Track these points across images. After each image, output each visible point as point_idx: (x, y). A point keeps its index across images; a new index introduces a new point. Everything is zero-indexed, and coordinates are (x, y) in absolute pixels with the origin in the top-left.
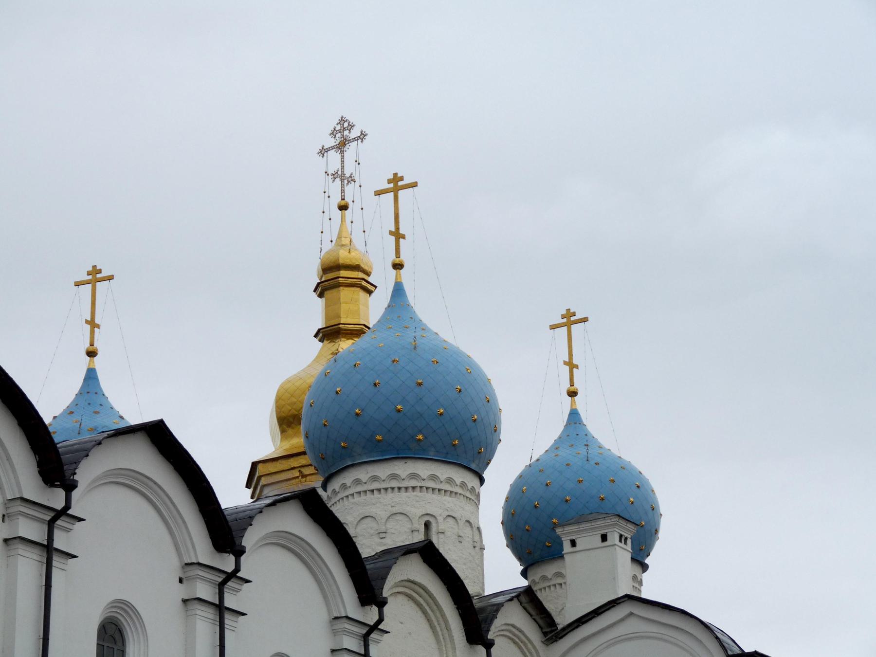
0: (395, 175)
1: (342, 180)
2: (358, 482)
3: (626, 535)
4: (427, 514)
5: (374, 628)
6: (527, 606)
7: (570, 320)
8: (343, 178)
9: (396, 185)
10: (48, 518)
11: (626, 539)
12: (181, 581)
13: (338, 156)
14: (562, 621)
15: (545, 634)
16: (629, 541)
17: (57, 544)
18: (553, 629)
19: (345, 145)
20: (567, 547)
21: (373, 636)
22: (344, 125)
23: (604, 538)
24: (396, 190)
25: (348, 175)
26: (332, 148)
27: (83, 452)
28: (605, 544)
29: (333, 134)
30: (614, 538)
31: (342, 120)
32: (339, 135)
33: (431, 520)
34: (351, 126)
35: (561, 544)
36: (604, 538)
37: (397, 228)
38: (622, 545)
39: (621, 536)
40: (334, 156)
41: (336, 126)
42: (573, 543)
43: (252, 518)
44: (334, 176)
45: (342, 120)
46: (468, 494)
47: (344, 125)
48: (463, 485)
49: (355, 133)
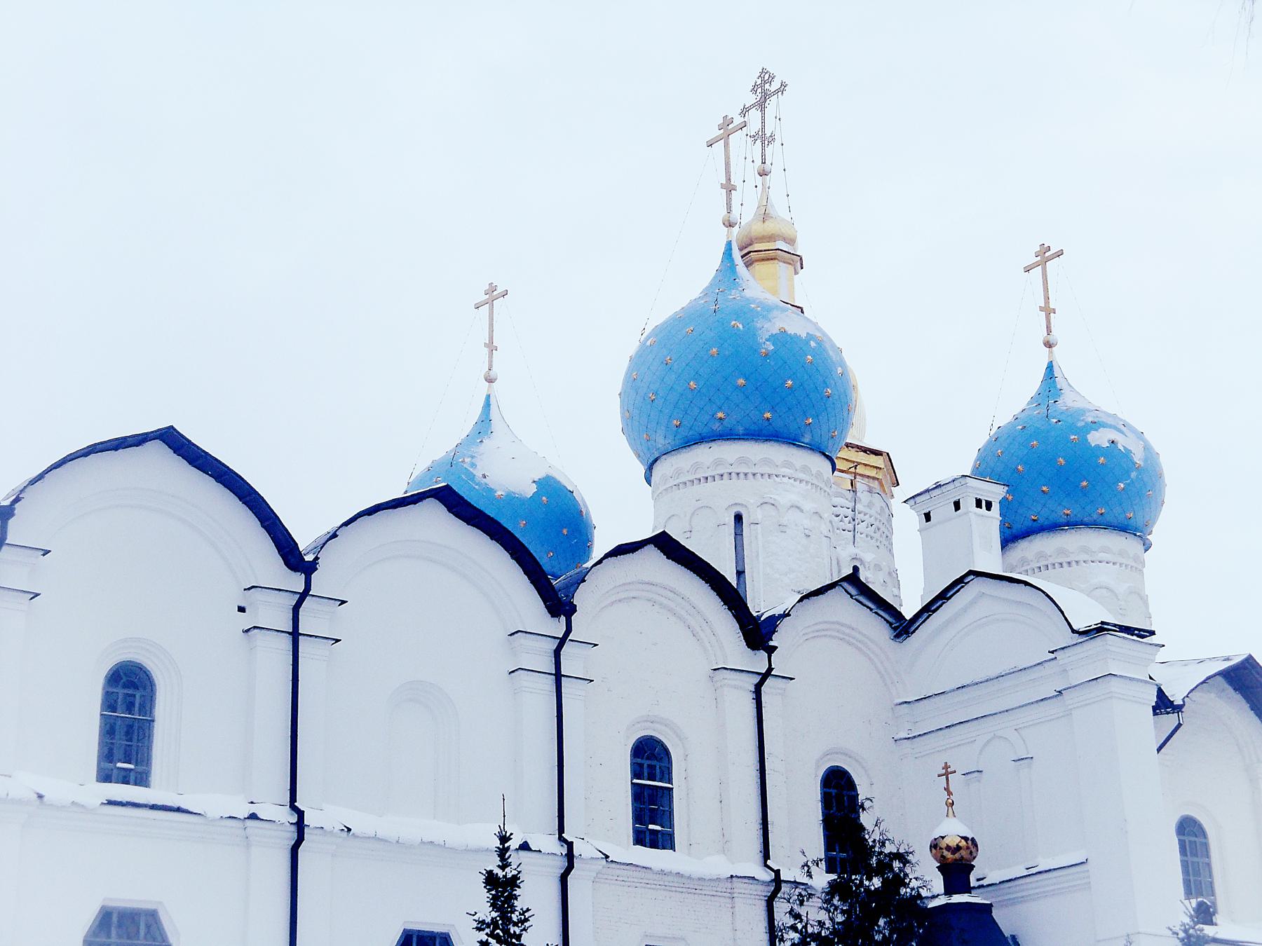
4: (736, 504)
6: (861, 598)
7: (1045, 256)
14: (908, 613)
15: (895, 629)
16: (996, 507)
18: (902, 622)
22: (766, 77)
23: (957, 505)
25: (768, 135)
29: (754, 90)
32: (759, 90)
34: (772, 78)
36: (957, 505)
39: (978, 503)
41: (757, 80)
45: (763, 71)
47: (766, 77)
49: (775, 85)
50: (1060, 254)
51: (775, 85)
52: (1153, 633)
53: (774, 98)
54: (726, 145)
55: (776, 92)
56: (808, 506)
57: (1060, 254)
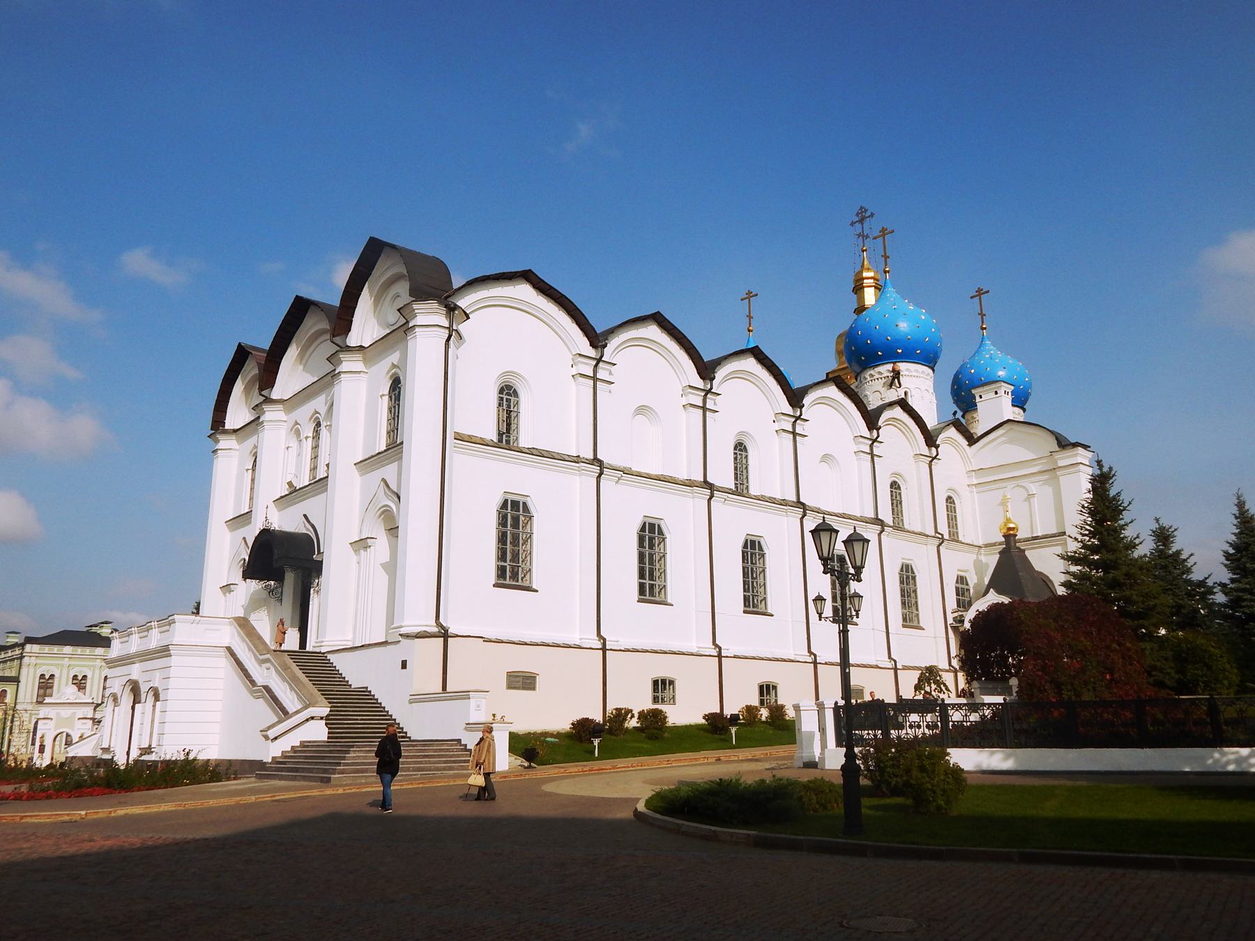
0: (883, 228)
1: (863, 237)
2: (872, 376)
3: (1007, 391)
5: (875, 441)
7: (980, 292)
8: (863, 236)
9: (884, 232)
10: (703, 394)
12: (774, 422)
13: (860, 225)
16: (1010, 394)
17: (708, 406)
19: (863, 220)
20: (978, 399)
21: (875, 444)
22: (863, 210)
23: (996, 393)
24: (884, 236)
26: (857, 222)
27: (718, 363)
28: (997, 396)
29: (857, 215)
30: (1001, 392)
31: (862, 208)
33: (908, 390)
34: (866, 211)
35: (975, 398)
36: (996, 393)
37: (885, 253)
38: (1006, 395)
40: (858, 225)
42: (981, 397)
43: (807, 391)
44: (859, 235)
45: (862, 208)
46: (926, 377)
47: (863, 210)
48: (923, 372)
49: (868, 214)
51: (868, 214)
52: (1089, 447)
53: (868, 219)
54: (884, 238)
55: (869, 217)
56: (923, 388)
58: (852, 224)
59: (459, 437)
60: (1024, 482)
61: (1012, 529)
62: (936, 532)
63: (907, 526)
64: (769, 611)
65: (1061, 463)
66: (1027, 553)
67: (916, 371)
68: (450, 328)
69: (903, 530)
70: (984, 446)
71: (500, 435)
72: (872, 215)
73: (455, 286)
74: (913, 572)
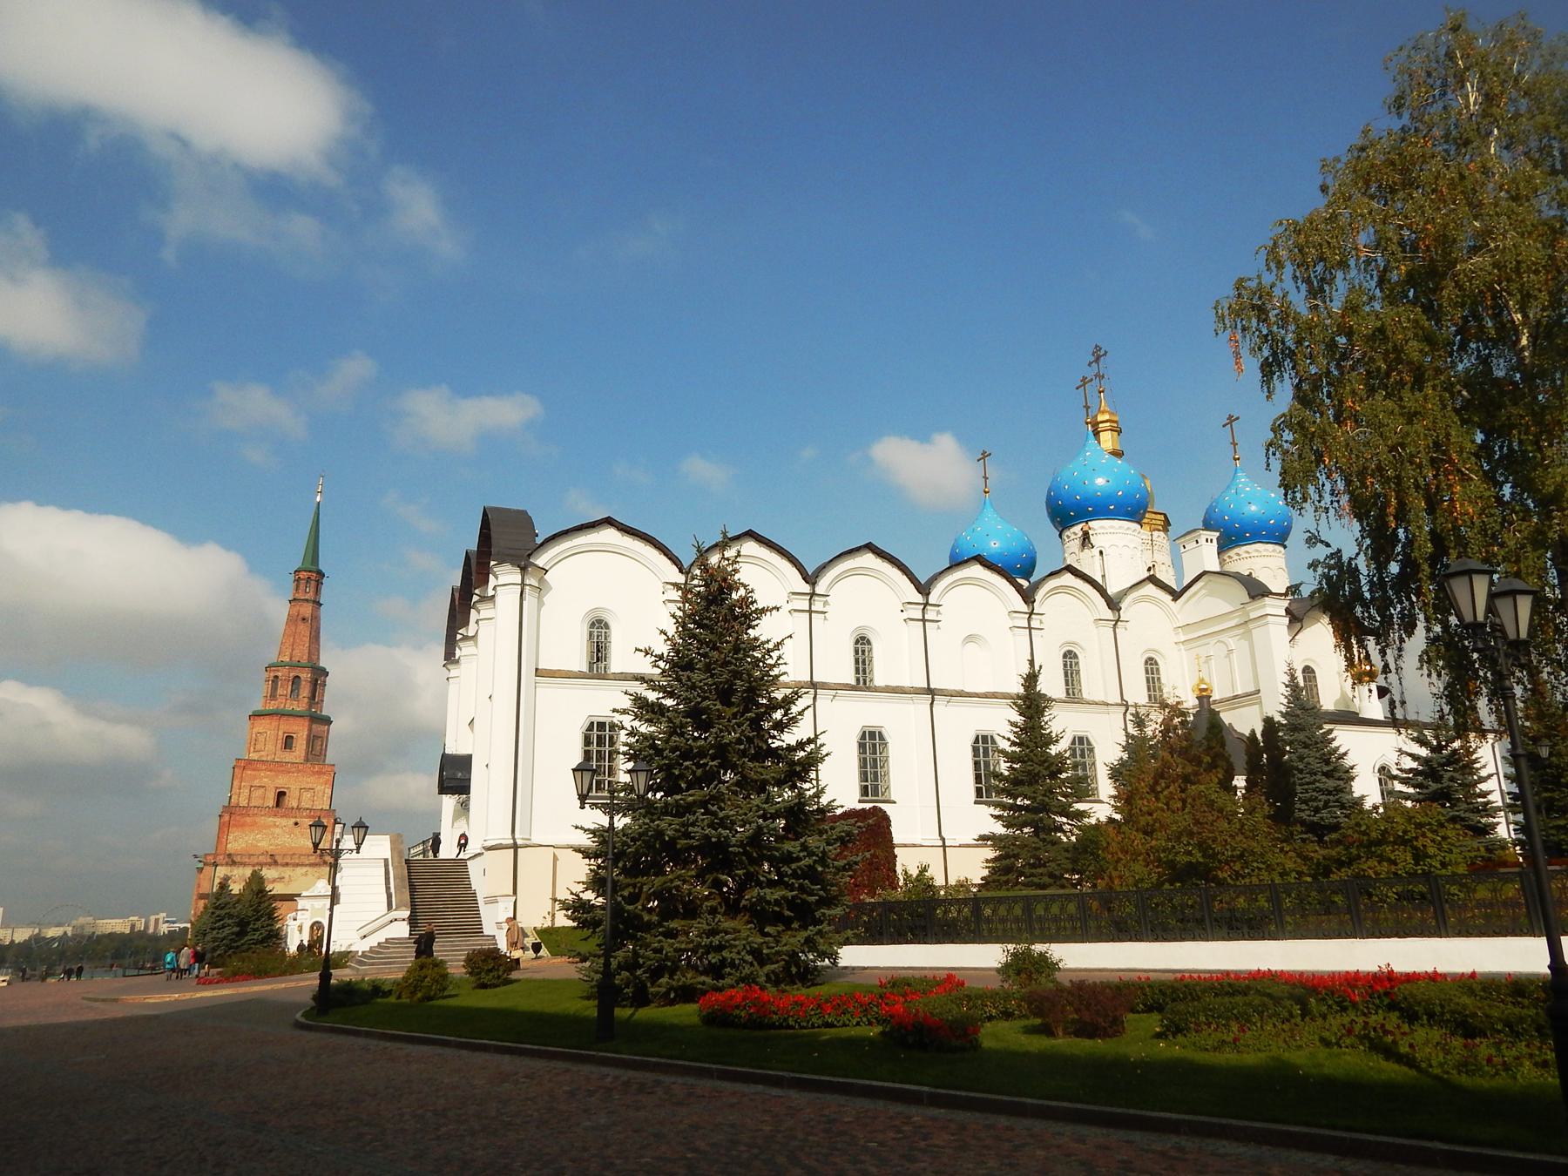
11: (1211, 541)
16: (1215, 541)
22: (1098, 348)
30: (1202, 540)
31: (1096, 346)
39: (1207, 540)
45: (1096, 346)
47: (1098, 348)
49: (1102, 352)
50: (1237, 418)
57: (1237, 418)
58: (1090, 364)
59: (539, 672)
60: (1223, 637)
61: (1205, 690)
62: (1122, 699)
63: (1085, 696)
64: (893, 798)
65: (1253, 615)
66: (1221, 715)
67: (1112, 527)
68: (523, 584)
69: (1081, 701)
70: (1188, 600)
71: (591, 664)
72: (1106, 352)
73: (539, 540)
74: (1089, 743)
